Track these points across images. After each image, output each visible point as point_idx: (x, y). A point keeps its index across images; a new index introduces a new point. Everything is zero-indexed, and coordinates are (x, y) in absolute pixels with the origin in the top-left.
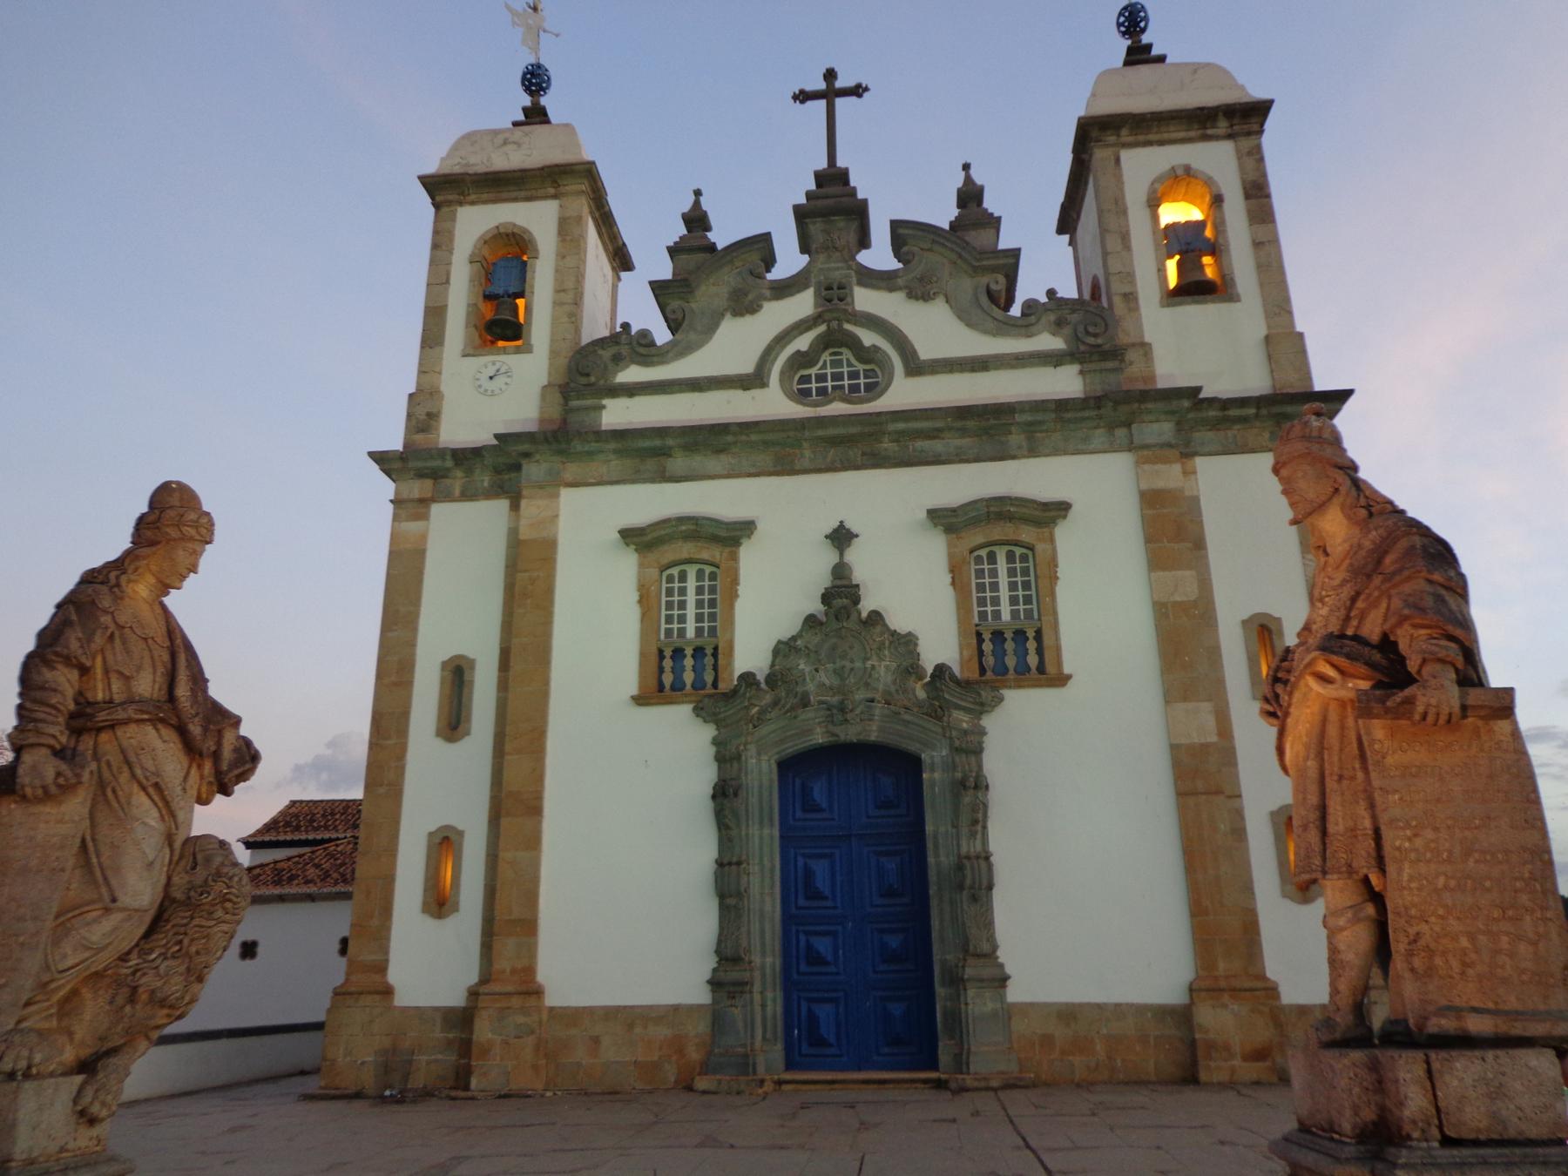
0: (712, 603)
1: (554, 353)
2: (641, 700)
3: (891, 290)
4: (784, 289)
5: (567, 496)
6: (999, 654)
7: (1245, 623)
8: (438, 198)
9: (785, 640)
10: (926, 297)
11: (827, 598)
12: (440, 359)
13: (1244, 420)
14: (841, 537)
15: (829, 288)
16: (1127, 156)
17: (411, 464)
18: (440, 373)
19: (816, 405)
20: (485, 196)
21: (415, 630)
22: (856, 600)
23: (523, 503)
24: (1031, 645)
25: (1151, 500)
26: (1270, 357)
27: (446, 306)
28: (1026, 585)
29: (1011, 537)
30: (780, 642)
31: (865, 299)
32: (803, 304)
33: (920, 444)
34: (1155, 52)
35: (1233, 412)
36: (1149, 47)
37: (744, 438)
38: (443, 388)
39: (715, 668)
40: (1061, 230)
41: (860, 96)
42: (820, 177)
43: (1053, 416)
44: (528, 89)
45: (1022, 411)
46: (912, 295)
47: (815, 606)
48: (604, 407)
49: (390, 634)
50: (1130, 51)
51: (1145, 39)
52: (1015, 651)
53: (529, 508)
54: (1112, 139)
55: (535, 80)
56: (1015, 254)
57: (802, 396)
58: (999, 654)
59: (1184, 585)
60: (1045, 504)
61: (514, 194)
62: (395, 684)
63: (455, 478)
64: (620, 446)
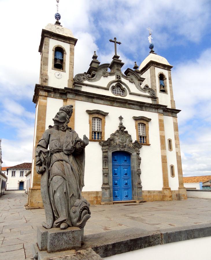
0: (100, 125)
1: (70, 74)
3: (127, 79)
4: (111, 74)
5: (77, 101)
6: (141, 140)
7: (168, 139)
8: (45, 35)
9: (114, 133)
10: (132, 82)
12: (48, 68)
13: (168, 111)
15: (118, 76)
16: (156, 68)
17: (44, 89)
18: (47, 71)
19: (116, 95)
20: (55, 38)
21: (45, 121)
23: (68, 101)
24: (145, 139)
26: (171, 103)
27: (48, 58)
28: (144, 130)
29: (143, 122)
30: (113, 134)
31: (123, 80)
32: (113, 78)
33: (131, 106)
35: (168, 110)
36: (153, 52)
37: (107, 98)
38: (48, 75)
39: (101, 136)
41: (120, 44)
43: (149, 106)
44: (56, 18)
45: (146, 104)
46: (130, 82)
47: (118, 129)
48: (82, 87)
49: (40, 121)
51: (153, 50)
52: (94, 135)
54: (154, 65)
55: (58, 17)
57: (113, 93)
60: (149, 119)
61: (61, 40)
62: (41, 131)
63: (52, 93)
64: (86, 95)
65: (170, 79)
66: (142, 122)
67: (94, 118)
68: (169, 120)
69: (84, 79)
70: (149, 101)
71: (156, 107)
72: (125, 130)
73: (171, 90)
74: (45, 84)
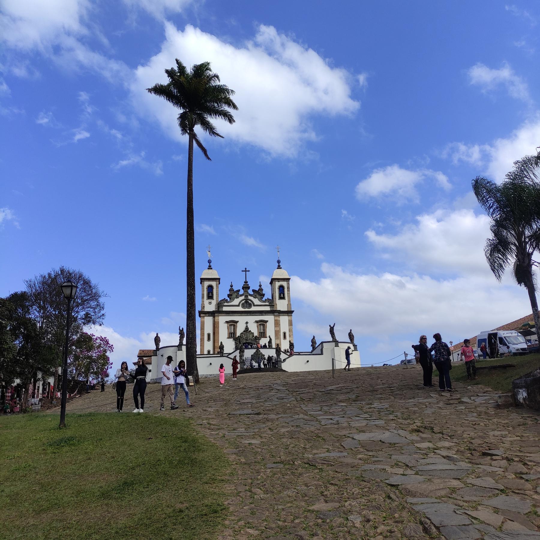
2: (228, 338)
4: (241, 295)
6: (261, 334)
10: (256, 298)
11: (246, 329)
14: (247, 323)
19: (245, 308)
22: (248, 329)
25: (275, 320)
31: (250, 297)
32: (243, 297)
34: (281, 267)
40: (270, 284)
42: (245, 282)
46: (254, 297)
50: (278, 266)
53: (216, 318)
56: (264, 294)
57: (243, 307)
58: (261, 334)
59: (278, 329)
65: (288, 288)
66: (262, 324)
67: (231, 325)
68: (284, 320)
69: (224, 302)
70: (268, 308)
71: (274, 312)
72: (249, 330)
73: (289, 296)
74: (203, 311)
